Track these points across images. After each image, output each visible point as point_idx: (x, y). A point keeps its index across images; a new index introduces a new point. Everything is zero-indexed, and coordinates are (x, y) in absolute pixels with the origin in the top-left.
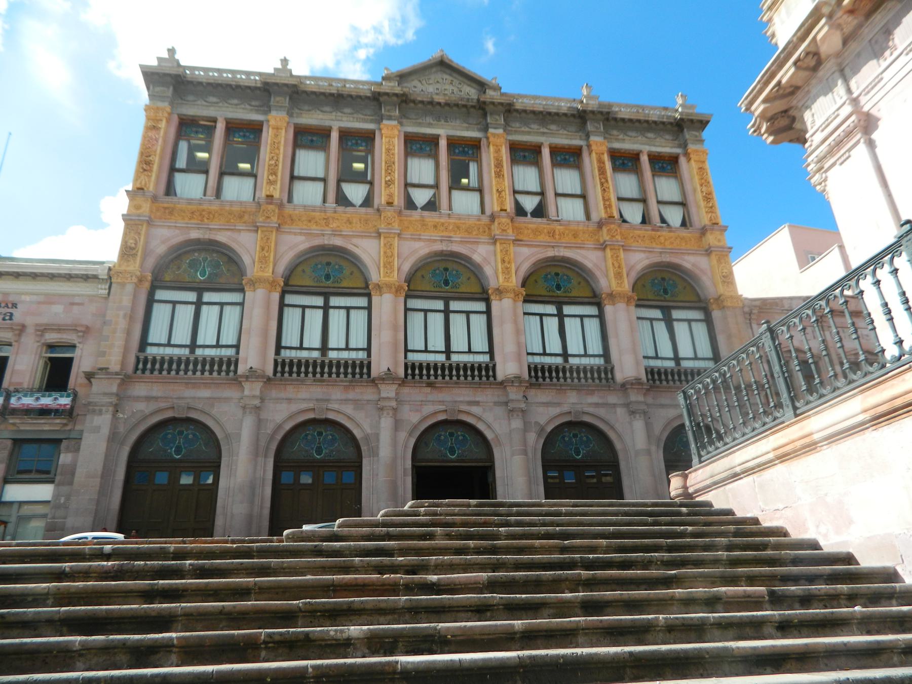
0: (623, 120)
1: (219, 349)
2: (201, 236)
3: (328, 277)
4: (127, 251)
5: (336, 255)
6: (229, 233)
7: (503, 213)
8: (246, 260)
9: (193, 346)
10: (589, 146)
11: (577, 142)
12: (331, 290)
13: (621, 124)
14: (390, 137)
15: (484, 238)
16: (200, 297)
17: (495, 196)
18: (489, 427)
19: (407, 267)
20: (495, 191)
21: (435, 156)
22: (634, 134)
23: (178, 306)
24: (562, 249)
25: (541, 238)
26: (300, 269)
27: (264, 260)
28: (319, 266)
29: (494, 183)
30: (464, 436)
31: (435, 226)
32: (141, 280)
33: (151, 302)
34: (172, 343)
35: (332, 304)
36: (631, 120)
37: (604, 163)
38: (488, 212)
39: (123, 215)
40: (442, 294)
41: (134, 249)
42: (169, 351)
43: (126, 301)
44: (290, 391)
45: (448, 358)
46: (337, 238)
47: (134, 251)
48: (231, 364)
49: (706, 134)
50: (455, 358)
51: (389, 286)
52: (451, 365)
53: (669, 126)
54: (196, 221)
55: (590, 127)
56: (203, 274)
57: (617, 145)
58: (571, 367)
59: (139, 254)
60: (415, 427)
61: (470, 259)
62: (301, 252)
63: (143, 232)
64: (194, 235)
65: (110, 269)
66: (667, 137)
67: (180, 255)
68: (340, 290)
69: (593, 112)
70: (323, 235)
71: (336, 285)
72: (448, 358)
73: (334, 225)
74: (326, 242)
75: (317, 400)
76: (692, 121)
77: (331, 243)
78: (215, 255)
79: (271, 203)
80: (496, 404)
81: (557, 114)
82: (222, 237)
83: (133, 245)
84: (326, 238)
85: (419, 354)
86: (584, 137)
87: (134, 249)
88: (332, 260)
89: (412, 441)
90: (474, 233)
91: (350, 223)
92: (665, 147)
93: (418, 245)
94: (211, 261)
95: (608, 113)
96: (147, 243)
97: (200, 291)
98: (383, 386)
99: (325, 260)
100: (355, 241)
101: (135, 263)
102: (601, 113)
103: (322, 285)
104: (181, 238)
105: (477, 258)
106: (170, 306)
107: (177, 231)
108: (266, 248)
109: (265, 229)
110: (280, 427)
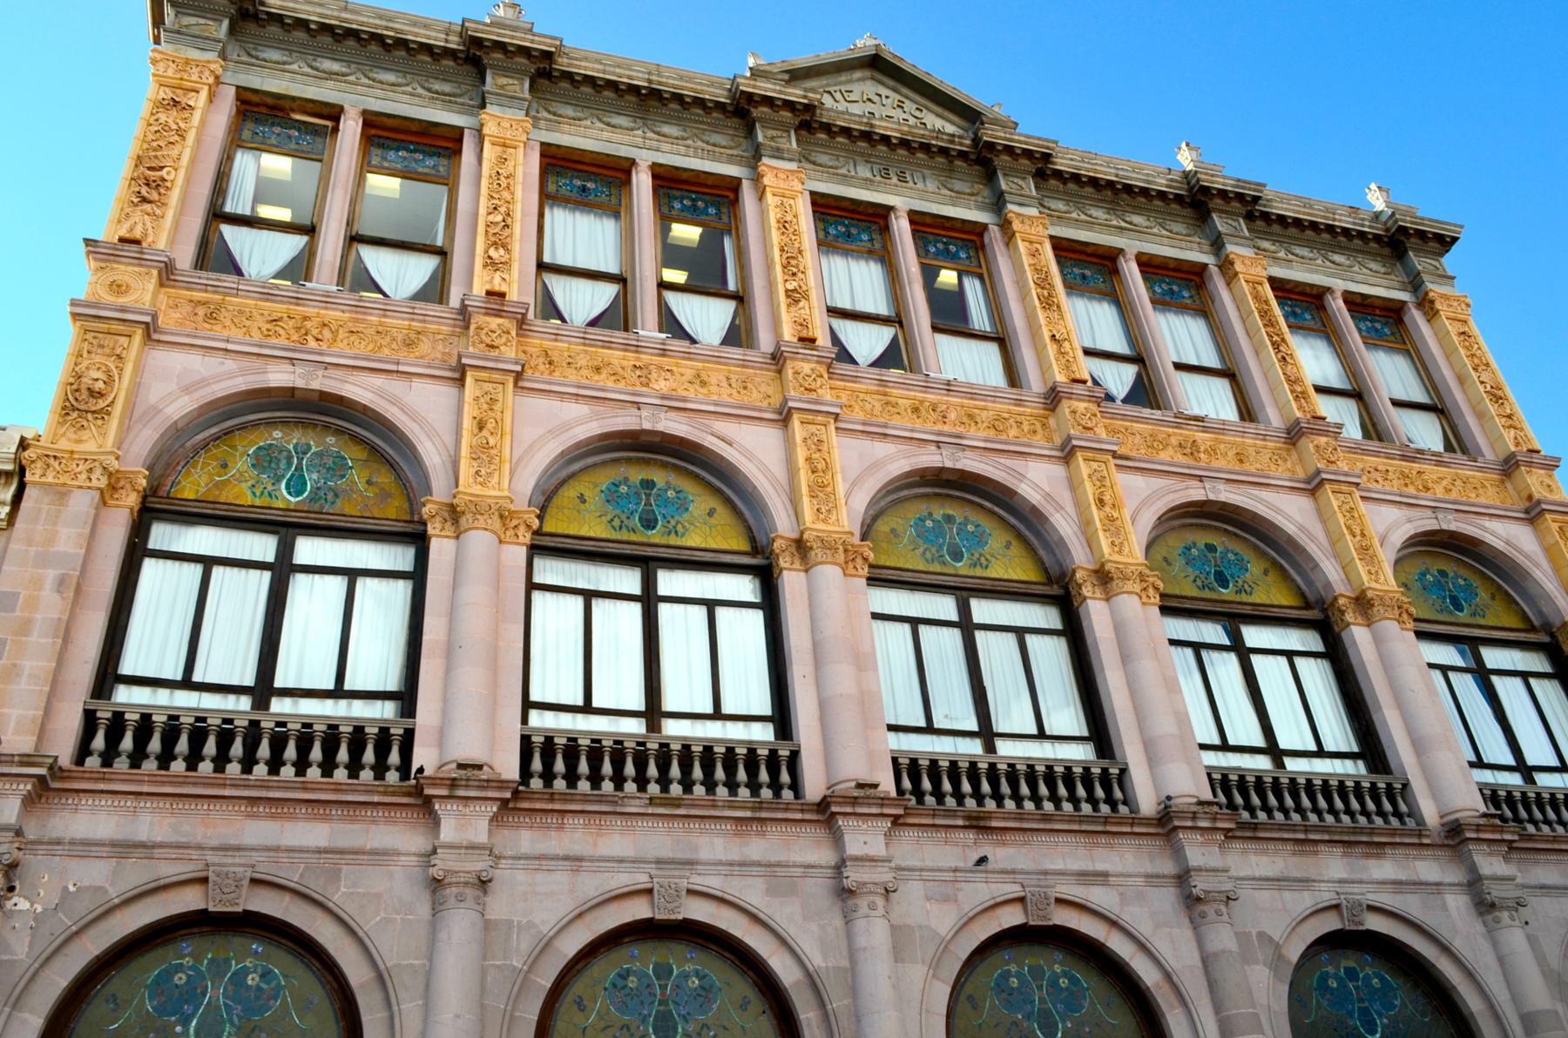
0: (1281, 219)
1: (343, 703)
2: (300, 383)
3: (649, 524)
4: (81, 402)
5: (664, 465)
6: (378, 381)
7: (1079, 389)
8: (432, 455)
9: (263, 689)
10: (1226, 266)
11: (1196, 254)
12: (663, 553)
13: (1276, 228)
14: (782, 196)
15: (1040, 444)
16: (285, 550)
17: (1051, 349)
18: (1143, 947)
19: (861, 501)
20: (1047, 340)
21: (886, 257)
22: (1304, 252)
23: (218, 572)
24: (1221, 486)
25: (1164, 456)
26: (570, 493)
27: (484, 452)
28: (624, 489)
29: (1042, 321)
30: (1072, 979)
31: (916, 410)
32: (115, 483)
33: (136, 553)
34: (197, 677)
35: (663, 590)
36: (1298, 222)
37: (1267, 302)
38: (1035, 383)
39: (74, 303)
40: (951, 581)
41: (101, 395)
42: (185, 699)
43: (68, 541)
44: (575, 837)
45: (990, 748)
46: (672, 414)
47: (101, 404)
48: (385, 749)
49: (1450, 261)
50: (1005, 749)
51: (828, 545)
52: (992, 766)
53: (1373, 245)
54: (283, 342)
55: (1220, 223)
56: (296, 486)
57: (1279, 272)
58: (1293, 780)
59: (117, 410)
60: (946, 946)
61: (1012, 493)
62: (578, 445)
63: (132, 356)
64: (279, 376)
65: (23, 444)
66: (1373, 265)
67: (228, 432)
68: (685, 555)
69: (1223, 194)
70: (638, 405)
71: (673, 540)
72: (990, 748)
73: (662, 385)
74: (647, 426)
75: (659, 862)
76: (1421, 234)
77: (660, 427)
78: (331, 440)
79: (498, 313)
80: (1152, 878)
81: (1145, 192)
82: (359, 389)
83: (100, 385)
84: (644, 413)
85: (913, 737)
86: (1207, 248)
87: (101, 395)
88: (659, 477)
89: (942, 992)
90: (1013, 432)
91: (703, 383)
92: (1379, 285)
93: (882, 449)
94: (319, 455)
95: (1256, 199)
96: (136, 386)
97: (286, 529)
98: (852, 822)
99: (637, 475)
100: (721, 426)
101: (104, 435)
102: (1240, 197)
103: (634, 538)
104: (241, 384)
105: (1024, 490)
106: (196, 570)
107: (230, 364)
108: (490, 425)
109: (484, 375)
110: (547, 945)
